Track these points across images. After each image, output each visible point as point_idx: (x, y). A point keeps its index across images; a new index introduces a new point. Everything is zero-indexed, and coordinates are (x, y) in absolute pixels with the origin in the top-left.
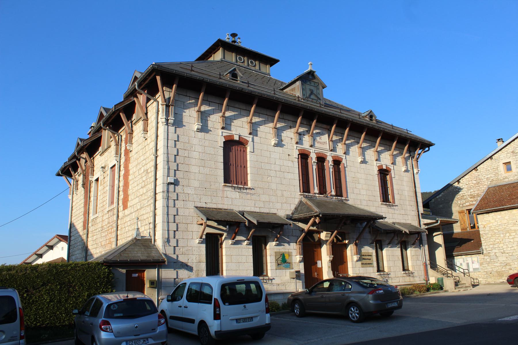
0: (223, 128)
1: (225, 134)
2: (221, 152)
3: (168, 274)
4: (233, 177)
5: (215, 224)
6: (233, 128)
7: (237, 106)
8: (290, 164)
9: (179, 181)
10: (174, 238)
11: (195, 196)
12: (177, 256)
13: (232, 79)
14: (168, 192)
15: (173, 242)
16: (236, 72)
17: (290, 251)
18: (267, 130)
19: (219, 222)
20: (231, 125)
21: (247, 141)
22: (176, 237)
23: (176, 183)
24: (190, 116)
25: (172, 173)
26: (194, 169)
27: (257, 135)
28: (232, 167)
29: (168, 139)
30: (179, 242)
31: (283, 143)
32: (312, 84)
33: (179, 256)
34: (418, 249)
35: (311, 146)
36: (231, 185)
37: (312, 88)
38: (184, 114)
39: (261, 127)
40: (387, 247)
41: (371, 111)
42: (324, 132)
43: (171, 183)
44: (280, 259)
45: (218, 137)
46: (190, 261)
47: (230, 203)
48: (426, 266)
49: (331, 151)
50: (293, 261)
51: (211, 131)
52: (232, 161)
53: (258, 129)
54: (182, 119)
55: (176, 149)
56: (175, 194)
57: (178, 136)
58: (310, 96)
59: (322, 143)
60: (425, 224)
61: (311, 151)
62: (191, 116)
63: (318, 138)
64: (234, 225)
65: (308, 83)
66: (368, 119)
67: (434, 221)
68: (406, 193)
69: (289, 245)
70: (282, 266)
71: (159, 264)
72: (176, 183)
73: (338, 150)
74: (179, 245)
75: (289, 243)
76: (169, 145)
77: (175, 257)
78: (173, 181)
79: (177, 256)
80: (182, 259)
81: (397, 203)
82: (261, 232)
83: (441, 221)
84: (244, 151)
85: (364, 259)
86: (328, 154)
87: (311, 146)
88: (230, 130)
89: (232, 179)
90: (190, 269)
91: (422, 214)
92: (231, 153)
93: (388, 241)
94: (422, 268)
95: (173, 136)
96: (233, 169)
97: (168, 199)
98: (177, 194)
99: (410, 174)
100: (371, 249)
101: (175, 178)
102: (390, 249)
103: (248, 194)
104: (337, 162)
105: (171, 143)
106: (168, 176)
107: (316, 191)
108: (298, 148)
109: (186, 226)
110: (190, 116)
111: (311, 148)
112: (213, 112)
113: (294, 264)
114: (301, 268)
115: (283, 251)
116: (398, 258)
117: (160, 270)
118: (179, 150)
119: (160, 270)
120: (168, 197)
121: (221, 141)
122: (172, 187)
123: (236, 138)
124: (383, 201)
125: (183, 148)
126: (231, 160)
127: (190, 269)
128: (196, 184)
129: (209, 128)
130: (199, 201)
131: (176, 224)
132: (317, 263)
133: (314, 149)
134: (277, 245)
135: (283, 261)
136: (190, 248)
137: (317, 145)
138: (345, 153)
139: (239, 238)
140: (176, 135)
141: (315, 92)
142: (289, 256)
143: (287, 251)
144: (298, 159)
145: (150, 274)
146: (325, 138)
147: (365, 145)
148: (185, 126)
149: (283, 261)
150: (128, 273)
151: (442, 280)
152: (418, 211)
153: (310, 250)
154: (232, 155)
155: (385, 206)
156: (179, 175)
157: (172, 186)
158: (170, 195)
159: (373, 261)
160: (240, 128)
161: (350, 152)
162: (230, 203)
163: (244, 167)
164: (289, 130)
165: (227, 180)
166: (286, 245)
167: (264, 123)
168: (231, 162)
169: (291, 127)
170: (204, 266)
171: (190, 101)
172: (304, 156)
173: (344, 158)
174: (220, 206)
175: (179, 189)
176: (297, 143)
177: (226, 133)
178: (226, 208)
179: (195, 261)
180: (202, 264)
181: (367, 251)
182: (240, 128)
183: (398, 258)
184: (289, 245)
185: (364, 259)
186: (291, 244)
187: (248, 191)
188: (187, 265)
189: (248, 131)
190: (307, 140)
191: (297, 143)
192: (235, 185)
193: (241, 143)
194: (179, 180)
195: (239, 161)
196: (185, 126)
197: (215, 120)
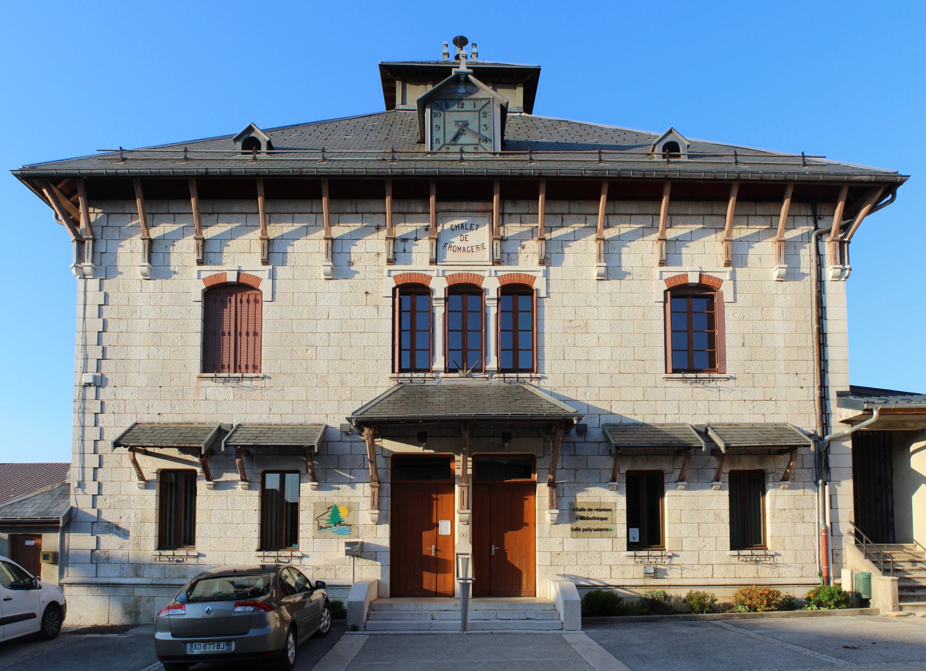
0: (200, 263)
1: (204, 275)
2: (197, 311)
3: (80, 542)
4: (227, 357)
5: (174, 452)
6: (226, 258)
7: (236, 208)
8: (369, 312)
9: (107, 380)
10: (94, 480)
11: (137, 402)
12: (99, 512)
13: (243, 153)
14: (84, 400)
15: (92, 488)
16: (253, 135)
17: (352, 500)
18: (308, 249)
19: (183, 450)
20: (221, 252)
21: (259, 280)
22: (99, 479)
23: (99, 383)
24: (132, 252)
25: (92, 365)
26: (139, 353)
27: (284, 264)
28: (226, 338)
29: (85, 305)
30: (104, 487)
31: (352, 268)
32: (468, 105)
33: (104, 511)
34: (809, 492)
35: (434, 262)
36: (213, 375)
37: (465, 117)
38: (120, 250)
39: (296, 243)
40: (675, 488)
41: (670, 132)
42: (478, 220)
43: (90, 385)
44: (327, 516)
45: (190, 281)
46: (123, 520)
47: (212, 410)
48: (831, 534)
49: (496, 262)
50: (361, 522)
51: (175, 273)
52: (228, 324)
53: (289, 249)
54: (116, 260)
55: (101, 320)
56: (99, 402)
57: (106, 295)
58: (455, 138)
59: (470, 249)
60: (846, 422)
61: (434, 274)
62: (130, 252)
63: (457, 241)
64: (221, 451)
65: (455, 108)
66: (656, 158)
67: (860, 412)
68: (780, 341)
69: (353, 488)
70: (329, 532)
71: (72, 521)
72: (99, 383)
73: (522, 258)
74: (104, 492)
75: (352, 483)
76: (87, 316)
77: (94, 513)
78: (90, 380)
79: (99, 512)
80: (107, 516)
81: (731, 368)
82: (277, 463)
83: (882, 412)
84: (256, 301)
85: (582, 518)
86: (486, 274)
87: (434, 262)
88: (220, 264)
89: (226, 363)
90: (123, 533)
91: (840, 394)
92: (226, 311)
93: (677, 473)
94: (815, 544)
95: (96, 297)
96: (228, 343)
97: (84, 413)
98: (102, 403)
99: (807, 287)
100: (614, 493)
101: (99, 374)
102: (686, 493)
103: (254, 388)
104: (517, 293)
105: (92, 311)
106: (85, 371)
107: (439, 363)
108: (393, 274)
109: (119, 458)
110: (132, 252)
111: (434, 267)
112: (182, 233)
113: (361, 528)
114: (381, 536)
115: (336, 501)
116: (717, 516)
117: (67, 534)
118: (109, 321)
119: (67, 534)
120: (84, 408)
121: (197, 290)
122: (91, 391)
123: (232, 278)
124: (675, 371)
125: (116, 316)
126: (226, 323)
127: (123, 533)
128: (142, 380)
129: (172, 269)
130: (145, 411)
131: (97, 456)
132: (437, 525)
133: (441, 268)
134: (319, 488)
135: (334, 520)
136: (125, 498)
137: (450, 256)
138: (542, 263)
139: (227, 477)
140: (102, 294)
141: (473, 126)
142: (350, 510)
143: (346, 500)
144: (394, 297)
145: (50, 541)
146: (481, 235)
147: (626, 230)
148: (121, 273)
149: (334, 520)
150: (13, 539)
151: (869, 578)
152: (823, 387)
153: (411, 494)
154: (228, 314)
155: (681, 384)
156: (106, 367)
157: (93, 389)
158: (87, 405)
159: (614, 523)
160: (241, 254)
161: (566, 256)
162: (212, 410)
163: (255, 334)
164: (375, 236)
165: (211, 362)
166: (345, 488)
167: (307, 231)
168: (226, 330)
169: (378, 228)
170: (151, 530)
171: (134, 223)
172: (411, 293)
173: (541, 274)
174: (189, 418)
175: (105, 393)
176: (390, 262)
177: (209, 271)
178: (202, 420)
179: (133, 520)
180: (147, 525)
181: (596, 500)
182: (241, 254)
183: (717, 516)
184: (353, 488)
185: (582, 518)
186: (358, 485)
187: (254, 383)
188: (117, 528)
189: (258, 257)
190: (422, 250)
191: (390, 262)
192: (232, 375)
193: (243, 287)
194: (107, 376)
195: (244, 324)
196: (121, 273)
197: (184, 250)
